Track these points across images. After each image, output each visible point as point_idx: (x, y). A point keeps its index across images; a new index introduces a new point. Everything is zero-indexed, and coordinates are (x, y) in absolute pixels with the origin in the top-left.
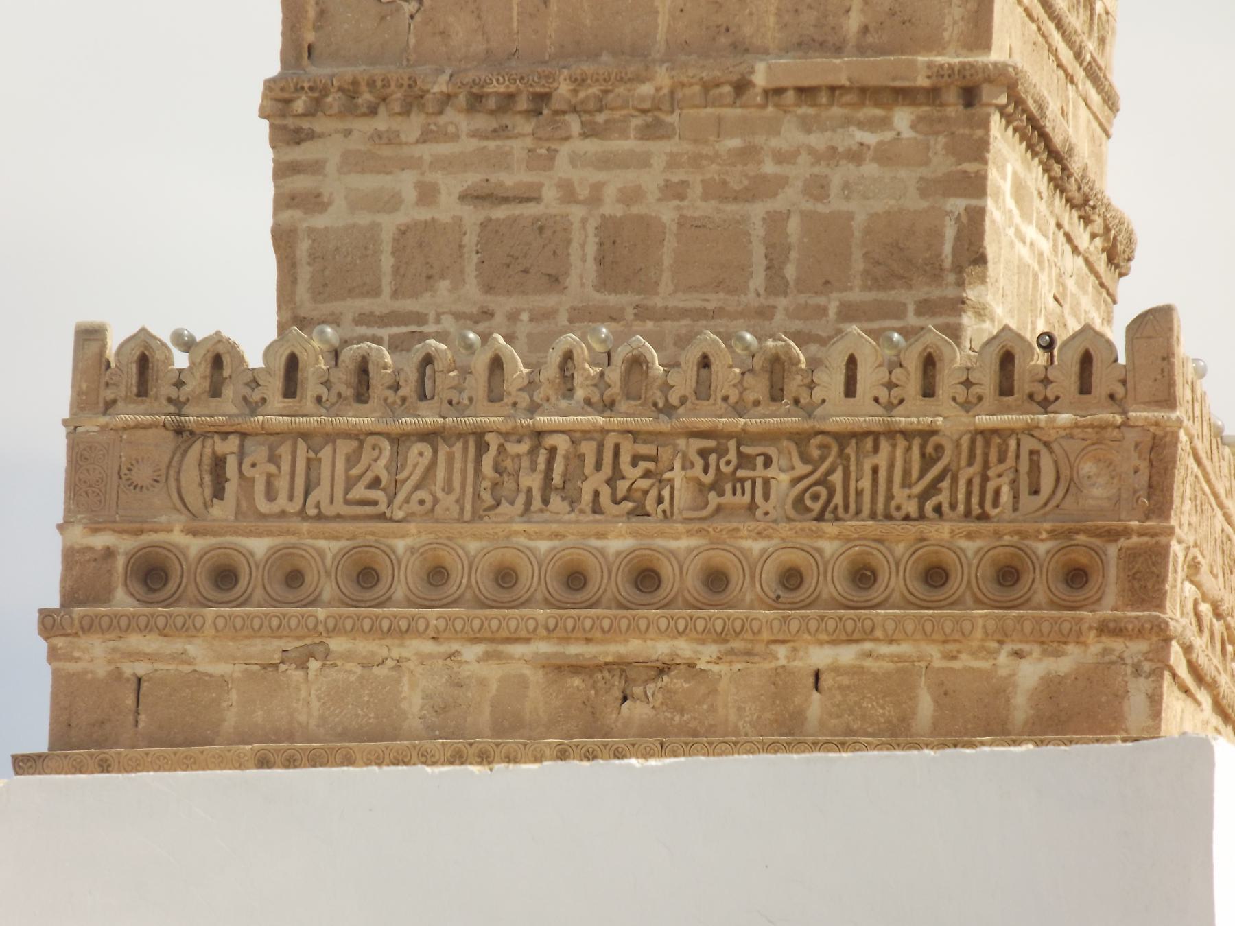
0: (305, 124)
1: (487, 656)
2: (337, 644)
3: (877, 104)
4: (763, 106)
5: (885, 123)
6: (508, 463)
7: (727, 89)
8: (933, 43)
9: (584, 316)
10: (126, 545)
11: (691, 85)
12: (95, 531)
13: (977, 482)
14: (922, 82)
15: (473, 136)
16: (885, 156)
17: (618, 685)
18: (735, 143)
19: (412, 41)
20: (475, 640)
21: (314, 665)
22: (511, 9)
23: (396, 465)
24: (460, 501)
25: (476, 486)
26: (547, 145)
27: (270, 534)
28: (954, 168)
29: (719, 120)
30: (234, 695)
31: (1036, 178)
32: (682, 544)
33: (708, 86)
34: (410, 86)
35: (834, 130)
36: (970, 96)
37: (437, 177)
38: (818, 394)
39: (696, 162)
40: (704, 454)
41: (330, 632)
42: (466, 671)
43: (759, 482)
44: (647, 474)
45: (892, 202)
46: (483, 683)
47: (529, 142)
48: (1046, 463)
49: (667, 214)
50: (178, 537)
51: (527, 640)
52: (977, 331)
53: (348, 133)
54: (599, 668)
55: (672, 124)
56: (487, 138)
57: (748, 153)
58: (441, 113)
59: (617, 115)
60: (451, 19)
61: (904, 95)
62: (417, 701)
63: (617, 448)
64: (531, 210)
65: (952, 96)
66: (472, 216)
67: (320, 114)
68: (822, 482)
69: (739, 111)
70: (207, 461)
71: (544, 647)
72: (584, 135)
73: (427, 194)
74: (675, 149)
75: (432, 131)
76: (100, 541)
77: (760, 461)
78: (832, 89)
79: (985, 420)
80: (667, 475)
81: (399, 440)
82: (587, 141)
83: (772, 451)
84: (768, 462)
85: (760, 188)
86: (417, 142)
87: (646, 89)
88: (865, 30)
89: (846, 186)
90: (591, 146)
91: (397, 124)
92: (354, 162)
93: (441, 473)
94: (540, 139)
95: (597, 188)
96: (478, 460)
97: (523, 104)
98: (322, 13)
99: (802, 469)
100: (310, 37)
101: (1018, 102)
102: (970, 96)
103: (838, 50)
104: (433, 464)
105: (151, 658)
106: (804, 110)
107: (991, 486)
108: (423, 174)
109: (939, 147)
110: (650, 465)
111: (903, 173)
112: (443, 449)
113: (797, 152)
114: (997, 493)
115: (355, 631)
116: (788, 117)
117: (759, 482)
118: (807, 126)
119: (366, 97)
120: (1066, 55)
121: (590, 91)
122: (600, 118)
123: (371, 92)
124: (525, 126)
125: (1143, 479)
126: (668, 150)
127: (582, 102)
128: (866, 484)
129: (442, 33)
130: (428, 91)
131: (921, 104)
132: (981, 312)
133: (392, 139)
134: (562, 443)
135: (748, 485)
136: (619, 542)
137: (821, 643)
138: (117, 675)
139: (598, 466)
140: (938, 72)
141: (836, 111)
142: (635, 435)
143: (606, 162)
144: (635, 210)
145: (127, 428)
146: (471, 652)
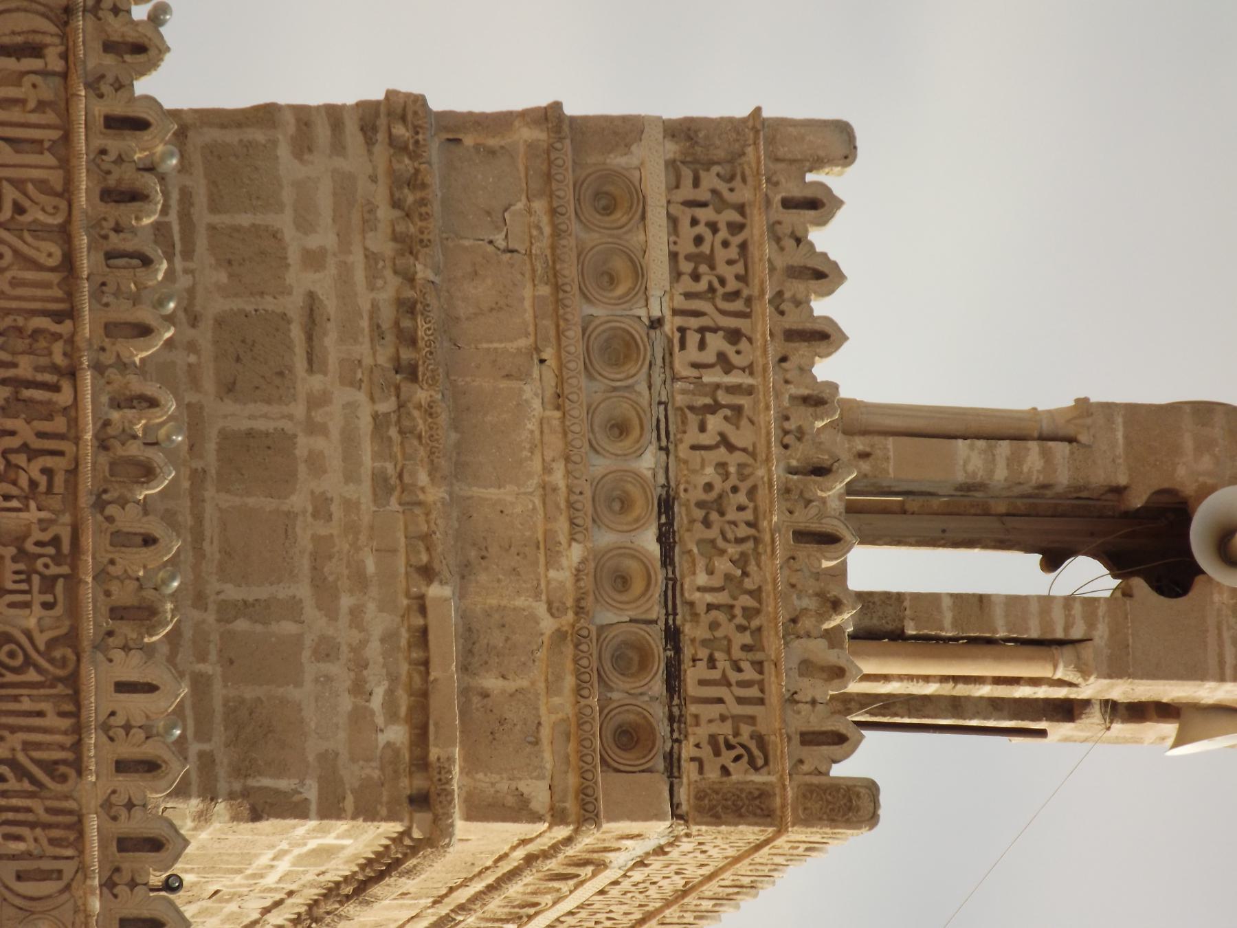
0: (381, 136)
3: (411, 710)
4: (408, 594)
5: (392, 717)
6: (42, 343)
7: (424, 558)
8: (472, 764)
9: (194, 419)
11: (428, 522)
13: (30, 817)
14: (434, 753)
15: (372, 305)
16: (360, 717)
18: (371, 567)
19: (466, 243)
22: (501, 341)
23: (38, 230)
25: (19, 311)
26: (366, 379)
28: (347, 786)
29: (394, 551)
31: (338, 869)
33: (426, 539)
34: (421, 241)
35: (384, 666)
36: (421, 802)
37: (332, 269)
38: (118, 655)
39: (351, 528)
40: (56, 541)
43: (27, 597)
44: (33, 484)
45: (313, 725)
47: (368, 361)
49: (298, 501)
52: (183, 814)
53: (374, 179)
55: (388, 504)
56: (371, 318)
57: (360, 581)
58: (396, 272)
59: (397, 449)
60: (489, 282)
61: (421, 735)
63: (61, 453)
64: (300, 364)
65: (420, 782)
66: (293, 304)
67: (392, 151)
68: (28, 662)
69: (402, 570)
70: (38, 38)
72: (375, 416)
73: (314, 259)
74: (363, 507)
75: (377, 263)
77: (49, 598)
78: (426, 663)
79: (93, 824)
80: (33, 505)
81: (64, 233)
82: (370, 419)
83: (59, 610)
84: (47, 606)
85: (325, 590)
86: (366, 249)
87: (423, 478)
88: (485, 695)
89: (329, 679)
90: (365, 423)
91: (384, 229)
92: (344, 187)
93: (30, 275)
94: (371, 372)
95: (322, 430)
97: (406, 355)
98: (492, 152)
99: (41, 640)
100: (469, 140)
101: (414, 849)
102: (420, 801)
103: (465, 668)
104: (39, 267)
106: (405, 635)
107: (25, 831)
108: (334, 255)
109: (368, 771)
110: (43, 487)
111: (342, 735)
112: (54, 278)
113: (361, 628)
114: (18, 838)
116: (398, 619)
117: (27, 597)
118: (389, 638)
119: (410, 198)
120: (462, 896)
121: (420, 421)
122: (393, 432)
123: (415, 201)
126: (363, 500)
127: (409, 414)
128: (26, 705)
129: (476, 273)
130: (417, 259)
131: (411, 751)
132: (203, 818)
133: (369, 223)
134: (64, 398)
135: (24, 586)
139: (41, 435)
140: (445, 768)
141: (404, 668)
142: (73, 472)
143: (349, 440)
144: (302, 469)
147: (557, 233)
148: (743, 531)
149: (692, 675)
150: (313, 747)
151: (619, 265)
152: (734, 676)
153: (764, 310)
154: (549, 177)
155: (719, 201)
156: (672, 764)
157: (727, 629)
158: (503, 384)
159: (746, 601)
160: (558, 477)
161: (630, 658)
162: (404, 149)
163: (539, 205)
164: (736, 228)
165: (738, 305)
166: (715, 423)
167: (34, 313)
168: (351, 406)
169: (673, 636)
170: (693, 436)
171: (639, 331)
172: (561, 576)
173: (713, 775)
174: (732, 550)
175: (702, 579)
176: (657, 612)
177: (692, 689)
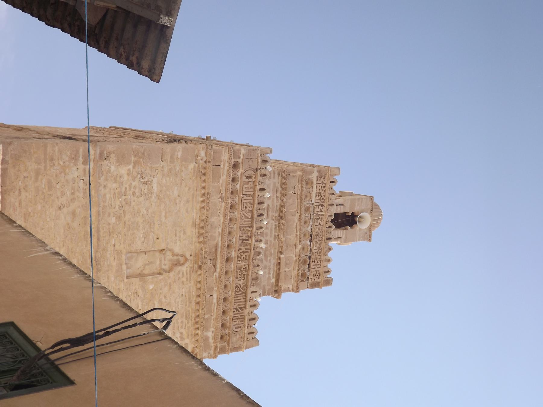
0: (280, 175)
1: (219, 233)
2: (223, 204)
6: (247, 232)
10: (240, 161)
12: (243, 155)
14: (280, 284)
16: (269, 278)
17: (212, 258)
20: (222, 231)
21: (220, 200)
24: (243, 224)
27: (240, 188)
30: (216, 184)
32: (232, 266)
33: (282, 247)
37: (271, 199)
39: (270, 245)
41: (226, 203)
42: (217, 229)
46: (215, 232)
48: (240, 329)
50: (241, 171)
51: (221, 240)
54: (216, 254)
57: (271, 254)
61: (277, 280)
62: (213, 220)
68: (240, 290)
71: (220, 244)
76: (242, 156)
81: (252, 211)
87: (282, 236)
90: (274, 227)
91: (279, 192)
92: (274, 184)
93: (247, 220)
96: (248, 227)
97: (281, 215)
98: (294, 176)
100: (291, 174)
105: (224, 168)
107: (237, 320)
112: (250, 220)
115: (226, 207)
118: (274, 263)
119: (284, 186)
124: (277, 215)
125: (235, 346)
128: (239, 298)
133: (277, 192)
134: (249, 242)
136: (234, 254)
137: (217, 296)
138: (221, 162)
142: (249, 255)
143: (271, 230)
144: (265, 236)
145: (258, 160)
146: (220, 230)
147: (302, 190)
148: (321, 239)
149: (312, 264)
150: (262, 284)
151: (308, 195)
152: (317, 264)
153: (326, 201)
154: (302, 181)
155: (323, 183)
156: (308, 279)
157: (317, 256)
158: (292, 217)
159: (320, 251)
160: (298, 233)
161: (305, 262)
162: (284, 177)
163: (300, 186)
164: (324, 187)
165: (323, 201)
166: (319, 221)
167: (246, 227)
168: (272, 223)
169: (310, 257)
170: (316, 224)
171: (310, 206)
172: (297, 250)
173: (313, 280)
174: (319, 242)
175: (315, 248)
176: (308, 254)
177: (312, 267)
